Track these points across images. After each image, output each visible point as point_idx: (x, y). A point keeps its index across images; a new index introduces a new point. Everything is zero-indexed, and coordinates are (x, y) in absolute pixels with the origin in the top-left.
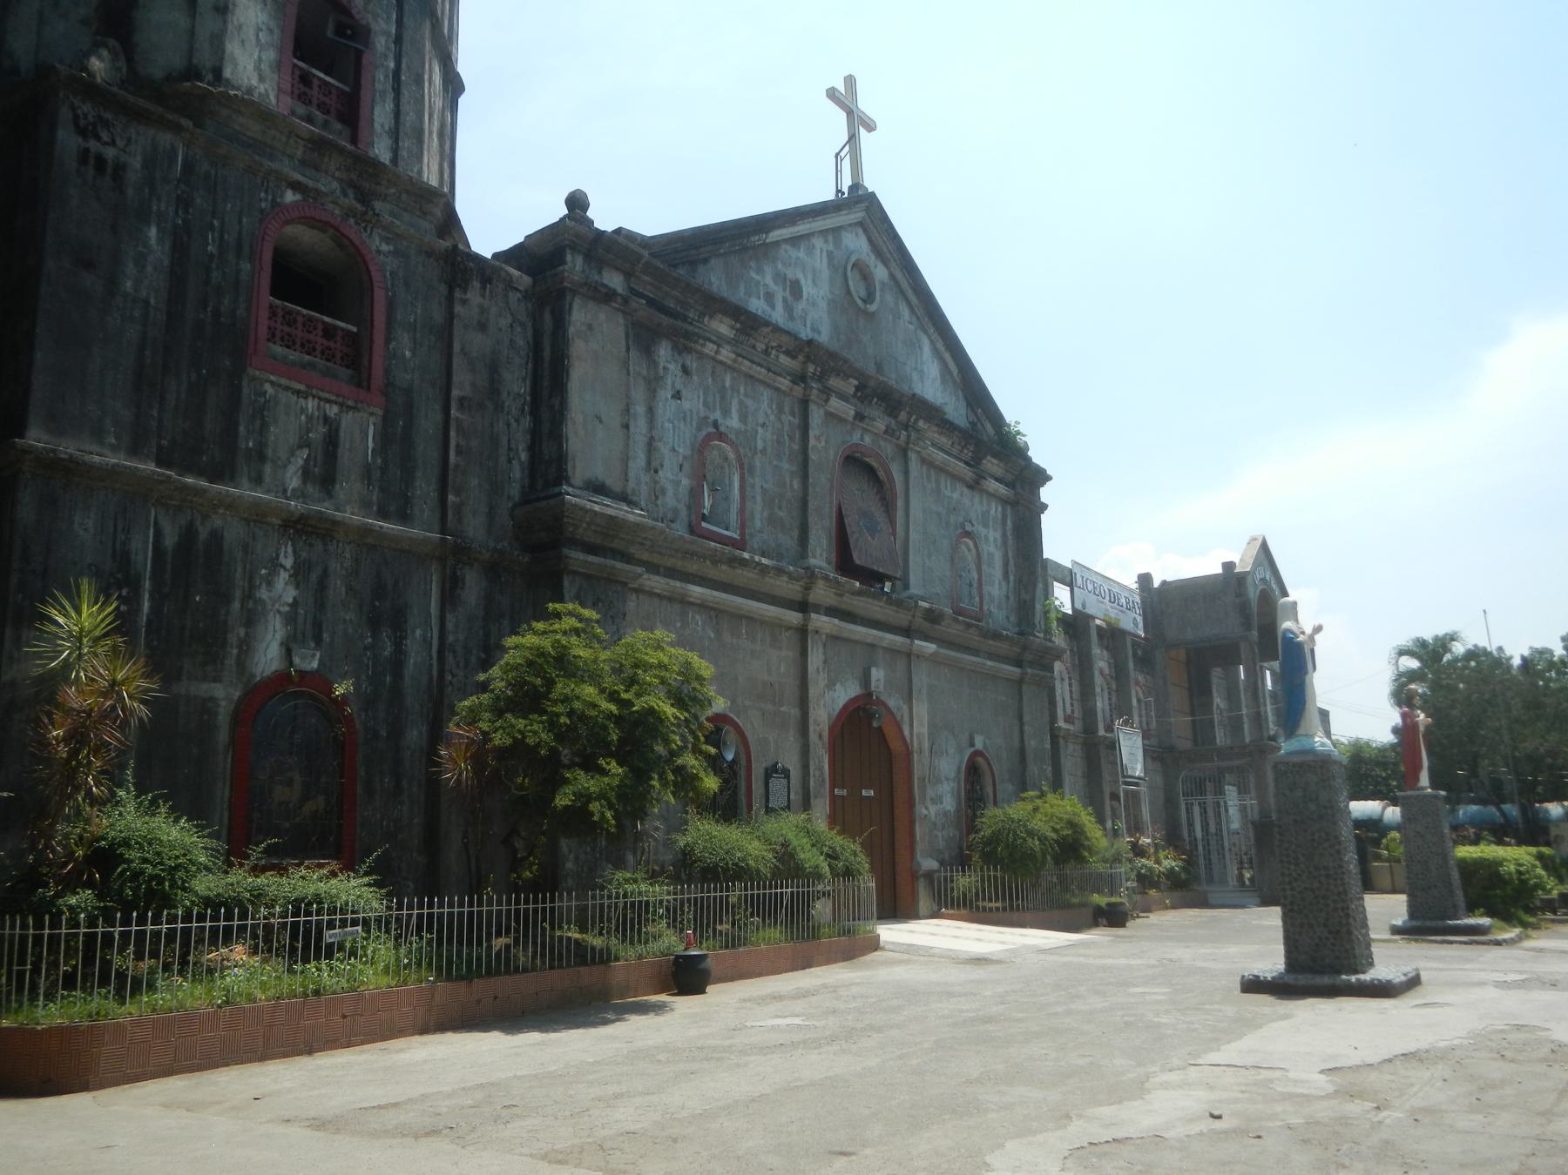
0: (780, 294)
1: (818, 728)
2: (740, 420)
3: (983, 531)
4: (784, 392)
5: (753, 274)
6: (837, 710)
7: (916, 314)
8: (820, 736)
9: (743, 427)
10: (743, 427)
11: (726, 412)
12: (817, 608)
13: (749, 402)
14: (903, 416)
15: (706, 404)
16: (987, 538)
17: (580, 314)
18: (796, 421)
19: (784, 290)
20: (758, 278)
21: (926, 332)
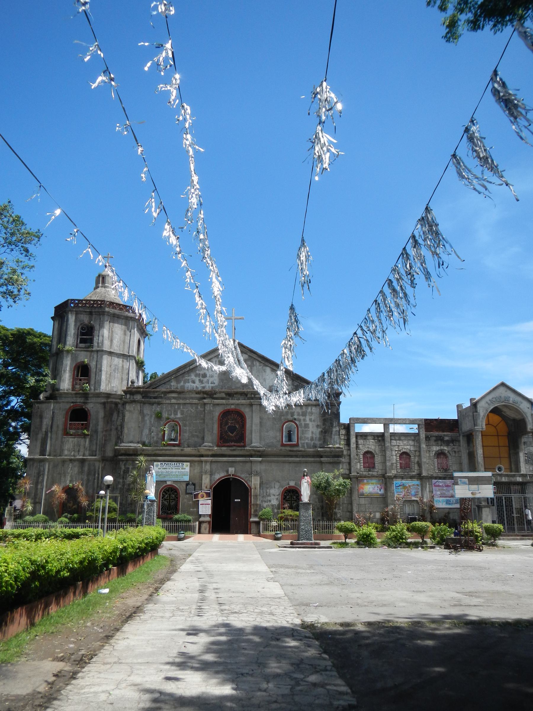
0: (197, 380)
1: (205, 485)
2: (181, 415)
3: (302, 418)
4: (198, 404)
5: (186, 378)
6: (216, 480)
7: (261, 362)
8: (206, 487)
9: (182, 416)
10: (182, 416)
11: (176, 414)
12: (207, 456)
13: (184, 410)
14: (249, 396)
15: (168, 415)
16: (304, 420)
17: (128, 407)
18: (203, 409)
19: (199, 377)
20: (189, 378)
21: (268, 366)
